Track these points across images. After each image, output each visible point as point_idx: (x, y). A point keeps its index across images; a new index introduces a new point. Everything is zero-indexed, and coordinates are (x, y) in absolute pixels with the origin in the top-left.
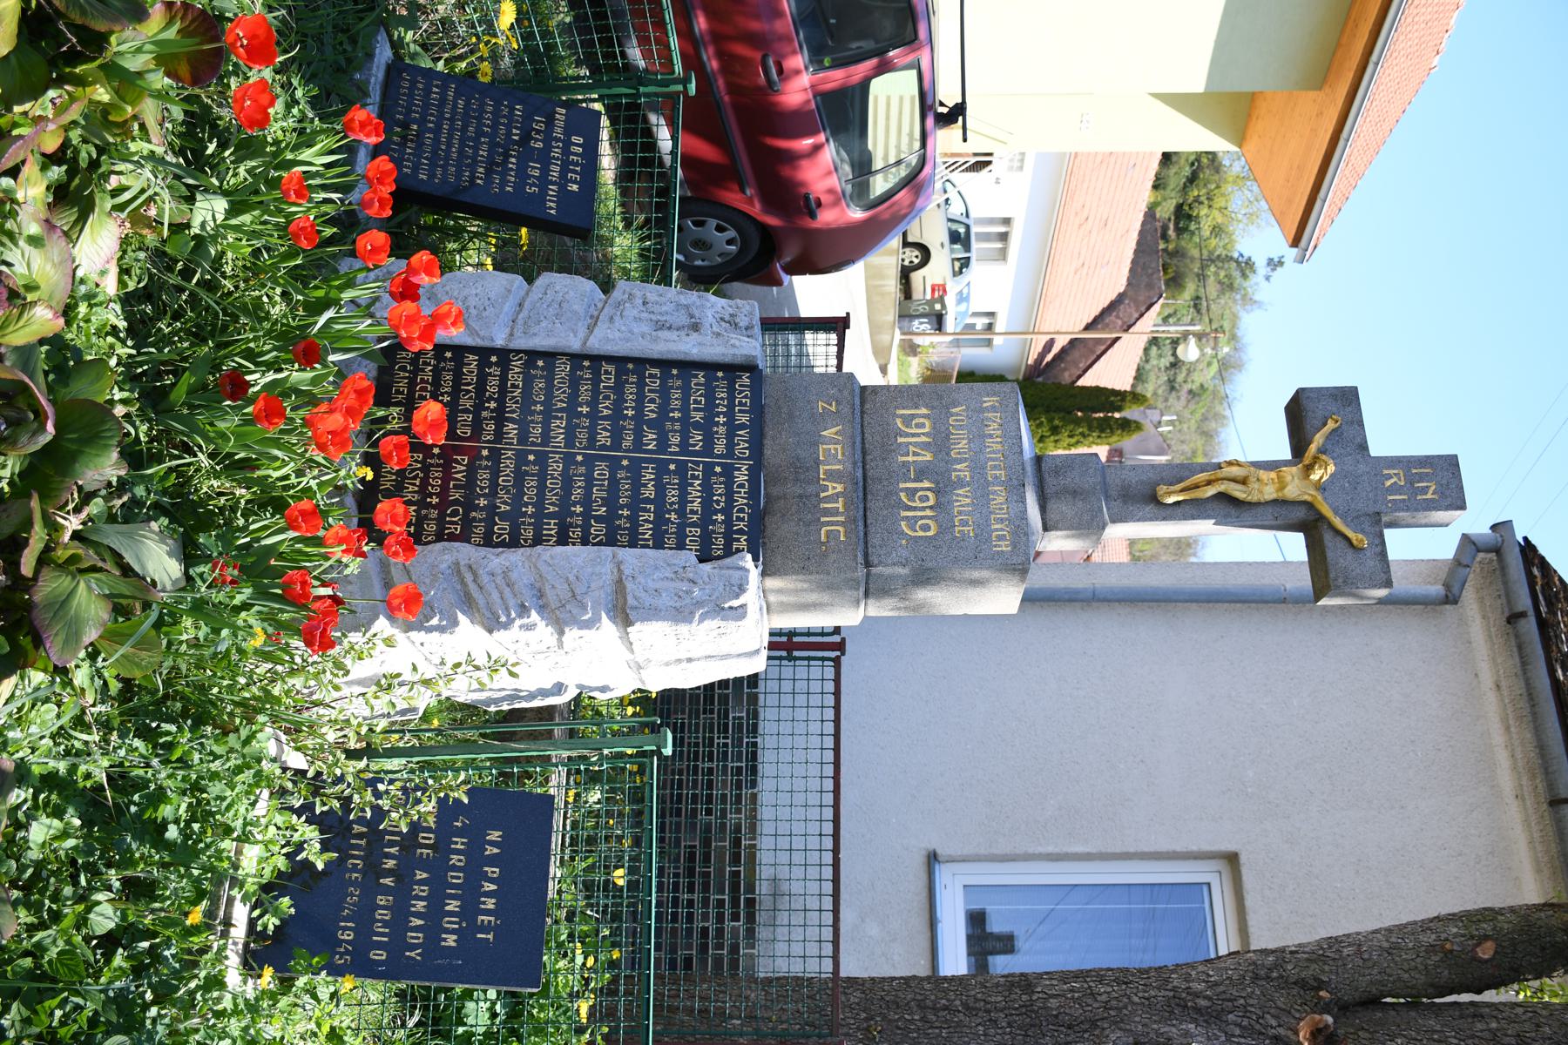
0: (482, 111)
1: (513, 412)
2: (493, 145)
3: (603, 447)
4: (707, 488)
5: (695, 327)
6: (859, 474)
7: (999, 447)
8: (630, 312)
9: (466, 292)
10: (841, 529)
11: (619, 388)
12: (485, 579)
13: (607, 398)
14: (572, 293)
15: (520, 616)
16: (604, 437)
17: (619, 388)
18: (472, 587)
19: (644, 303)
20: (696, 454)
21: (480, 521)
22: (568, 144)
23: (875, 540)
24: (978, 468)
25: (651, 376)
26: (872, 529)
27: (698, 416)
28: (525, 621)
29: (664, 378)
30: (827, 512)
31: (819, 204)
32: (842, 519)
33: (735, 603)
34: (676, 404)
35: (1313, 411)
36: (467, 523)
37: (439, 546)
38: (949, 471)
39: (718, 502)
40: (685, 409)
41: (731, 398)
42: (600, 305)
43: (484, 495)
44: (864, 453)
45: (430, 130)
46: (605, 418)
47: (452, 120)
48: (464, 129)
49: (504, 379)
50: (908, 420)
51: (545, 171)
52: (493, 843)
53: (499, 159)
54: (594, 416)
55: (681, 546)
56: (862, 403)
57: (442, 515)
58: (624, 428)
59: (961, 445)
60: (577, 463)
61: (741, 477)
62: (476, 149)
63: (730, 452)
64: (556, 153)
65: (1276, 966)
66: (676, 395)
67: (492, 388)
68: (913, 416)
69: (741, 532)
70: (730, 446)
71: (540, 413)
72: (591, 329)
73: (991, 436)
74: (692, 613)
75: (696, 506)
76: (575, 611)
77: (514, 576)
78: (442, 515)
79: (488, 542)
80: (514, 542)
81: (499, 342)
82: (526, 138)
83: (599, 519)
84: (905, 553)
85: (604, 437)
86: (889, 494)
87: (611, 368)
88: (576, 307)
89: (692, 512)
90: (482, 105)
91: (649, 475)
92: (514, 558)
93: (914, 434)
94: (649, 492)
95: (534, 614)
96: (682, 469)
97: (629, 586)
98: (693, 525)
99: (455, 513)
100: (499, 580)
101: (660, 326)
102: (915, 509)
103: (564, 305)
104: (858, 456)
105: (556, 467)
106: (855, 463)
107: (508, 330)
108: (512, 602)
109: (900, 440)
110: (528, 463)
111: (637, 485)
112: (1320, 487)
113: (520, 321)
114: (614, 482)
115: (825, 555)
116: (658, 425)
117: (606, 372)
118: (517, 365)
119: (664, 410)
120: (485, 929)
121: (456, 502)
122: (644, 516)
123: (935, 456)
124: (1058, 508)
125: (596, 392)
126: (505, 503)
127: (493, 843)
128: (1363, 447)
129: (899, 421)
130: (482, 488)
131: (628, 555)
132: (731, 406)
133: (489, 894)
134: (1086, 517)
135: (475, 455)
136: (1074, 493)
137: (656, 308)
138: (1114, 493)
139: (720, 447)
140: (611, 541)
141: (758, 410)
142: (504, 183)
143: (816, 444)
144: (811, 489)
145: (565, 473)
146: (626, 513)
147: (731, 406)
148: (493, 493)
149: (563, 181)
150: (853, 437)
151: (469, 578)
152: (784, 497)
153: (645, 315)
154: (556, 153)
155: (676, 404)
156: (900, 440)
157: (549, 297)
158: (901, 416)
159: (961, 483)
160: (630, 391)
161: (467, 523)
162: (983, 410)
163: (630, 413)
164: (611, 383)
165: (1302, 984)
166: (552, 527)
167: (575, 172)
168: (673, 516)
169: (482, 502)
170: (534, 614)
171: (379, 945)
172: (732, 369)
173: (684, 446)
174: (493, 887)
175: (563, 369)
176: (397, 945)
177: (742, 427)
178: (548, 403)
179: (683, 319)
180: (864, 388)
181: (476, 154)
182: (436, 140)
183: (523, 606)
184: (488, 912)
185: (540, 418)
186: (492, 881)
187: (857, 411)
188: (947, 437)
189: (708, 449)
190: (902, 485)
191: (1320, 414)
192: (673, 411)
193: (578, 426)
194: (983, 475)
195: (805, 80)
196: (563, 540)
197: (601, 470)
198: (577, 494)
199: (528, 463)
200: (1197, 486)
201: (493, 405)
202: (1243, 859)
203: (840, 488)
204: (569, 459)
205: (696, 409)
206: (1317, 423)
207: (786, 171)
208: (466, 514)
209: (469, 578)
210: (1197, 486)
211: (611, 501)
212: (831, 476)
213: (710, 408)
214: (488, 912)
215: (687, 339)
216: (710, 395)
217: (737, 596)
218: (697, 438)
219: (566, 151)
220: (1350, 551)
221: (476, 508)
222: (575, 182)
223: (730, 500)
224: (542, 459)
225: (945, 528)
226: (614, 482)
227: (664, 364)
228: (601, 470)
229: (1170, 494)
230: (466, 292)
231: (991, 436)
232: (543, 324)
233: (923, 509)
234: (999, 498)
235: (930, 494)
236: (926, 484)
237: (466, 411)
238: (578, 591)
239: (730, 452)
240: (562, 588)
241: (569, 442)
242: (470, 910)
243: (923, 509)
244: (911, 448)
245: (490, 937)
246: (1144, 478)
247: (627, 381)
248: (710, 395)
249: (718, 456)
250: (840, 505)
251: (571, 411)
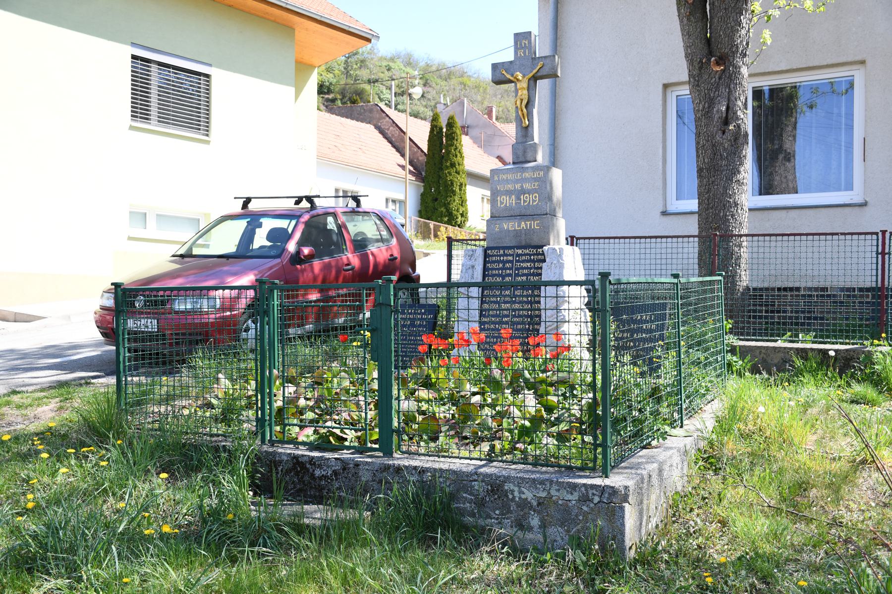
4: (523, 261)
5: (473, 267)
23: (539, 212)
24: (517, 181)
27: (501, 265)
29: (488, 275)
31: (392, 255)
41: (495, 256)
50: (502, 203)
55: (541, 268)
59: (510, 187)
61: (520, 251)
63: (513, 255)
65: (694, 78)
66: (494, 272)
70: (510, 255)
75: (529, 264)
93: (506, 201)
96: (517, 269)
105: (517, 306)
112: (524, 76)
116: (503, 277)
124: (529, 158)
128: (511, 62)
132: (497, 256)
136: (525, 152)
139: (511, 258)
141: (499, 248)
143: (509, 231)
147: (497, 256)
159: (522, 186)
165: (700, 68)
172: (486, 255)
173: (510, 269)
175: (486, 306)
189: (511, 262)
195: (350, 255)
198: (525, 299)
202: (666, 82)
207: (380, 268)
212: (519, 226)
213: (498, 262)
216: (494, 262)
218: (507, 265)
223: (527, 254)
224: (514, 310)
225: (535, 191)
234: (527, 175)
239: (513, 255)
248: (494, 262)
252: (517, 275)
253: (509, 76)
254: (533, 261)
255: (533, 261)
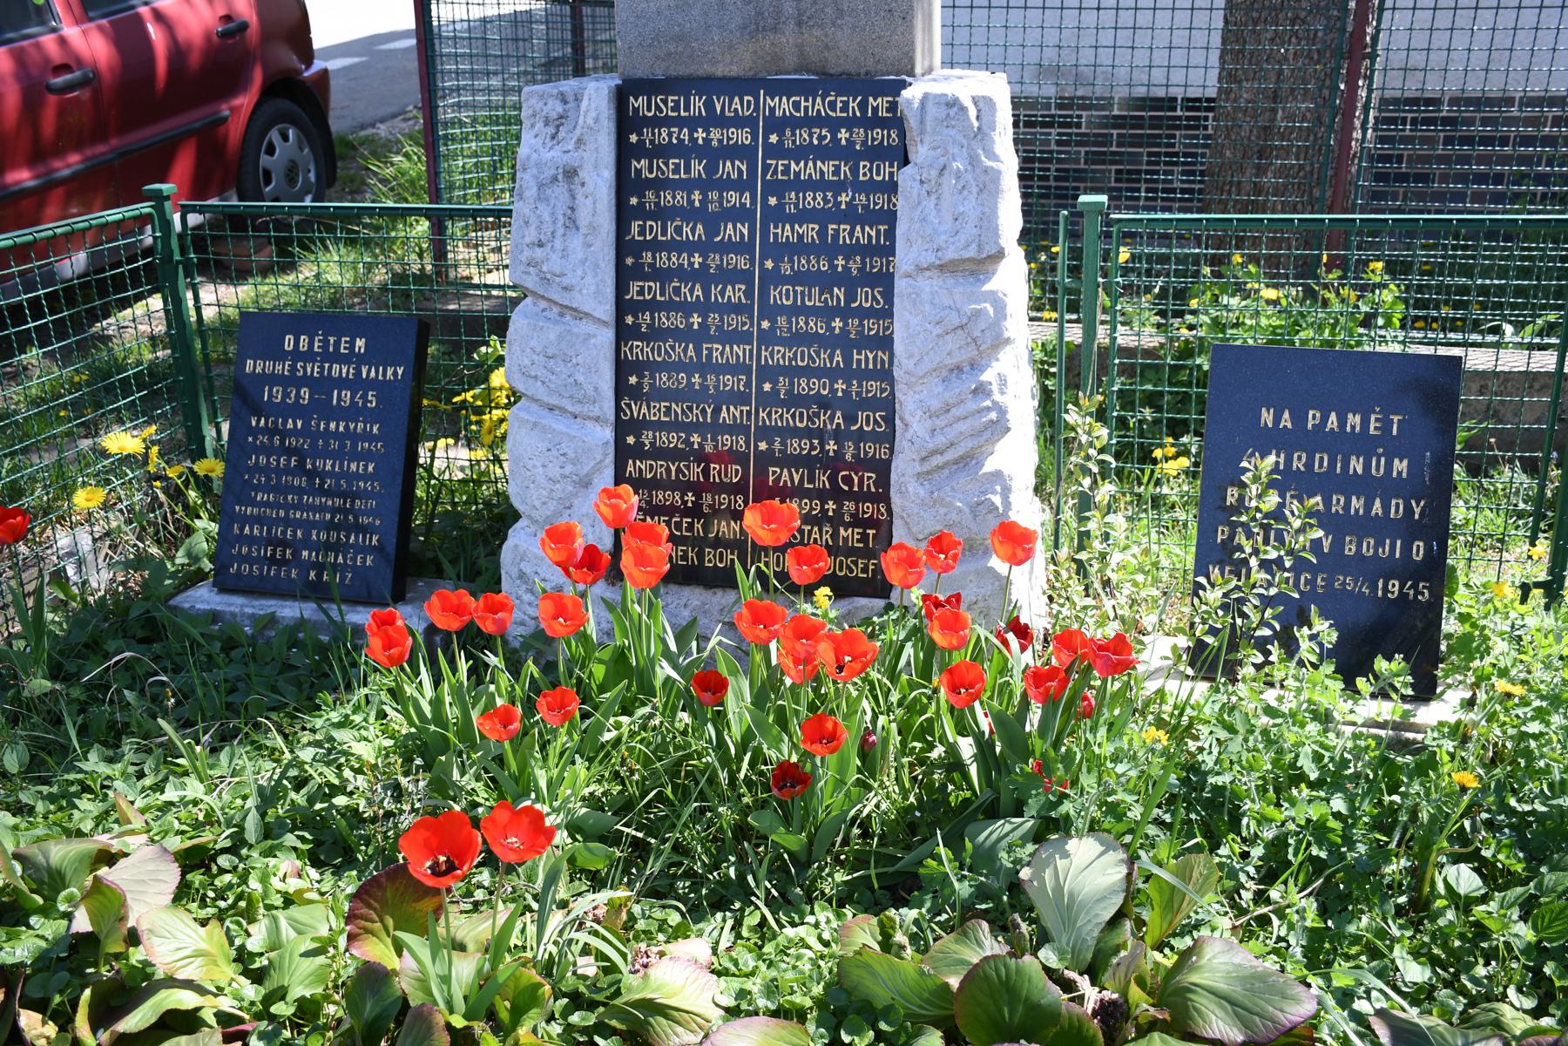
0: (265, 470)
1: (704, 411)
3: (749, 294)
4: (801, 153)
5: (571, 174)
8: (554, 263)
9: (541, 479)
11: (662, 276)
12: (940, 440)
13: (677, 291)
15: (989, 394)
16: (735, 293)
17: (662, 276)
18: (950, 455)
19: (541, 245)
22: (296, 355)
25: (642, 232)
27: (697, 168)
28: (995, 388)
29: (641, 213)
31: (227, 18)
33: (972, 112)
34: (681, 198)
37: (896, 499)
39: (821, 138)
40: (688, 186)
41: (667, 122)
42: (543, 304)
43: (822, 444)
45: (307, 535)
47: (288, 507)
48: (300, 491)
49: (659, 426)
51: (342, 383)
54: (704, 308)
55: (891, 187)
57: (850, 495)
58: (719, 267)
60: (773, 328)
61: (783, 106)
63: (750, 122)
64: (313, 369)
67: (672, 440)
70: (738, 122)
72: (580, 315)
74: (986, 170)
75: (827, 168)
76: (983, 325)
77: (935, 404)
78: (850, 495)
79: (889, 437)
80: (888, 406)
81: (608, 434)
82: (296, 410)
83: (851, 297)
85: (735, 293)
87: (634, 287)
88: (552, 336)
91: (786, 232)
92: (910, 404)
95: (985, 377)
96: (773, 187)
97: (950, 255)
98: (855, 171)
100: (939, 422)
101: (572, 223)
103: (550, 352)
105: (780, 355)
107: (589, 424)
108: (971, 406)
110: (775, 391)
111: (800, 248)
113: (576, 409)
114: (798, 278)
117: (641, 292)
118: (637, 410)
119: (690, 214)
120: (1386, 425)
121: (833, 479)
125: (669, 306)
126: (832, 418)
130: (812, 448)
131: (904, 259)
132: (680, 122)
133: (1342, 422)
135: (765, 460)
139: (742, 136)
140: (885, 281)
145: (787, 343)
146: (840, 262)
147: (680, 122)
148: (821, 434)
149: (350, 358)
151: (938, 460)
152: (800, 47)
153: (558, 244)
154: (313, 369)
157: (541, 372)
160: (664, 260)
161: (860, 464)
163: (697, 259)
166: (865, 358)
167: (337, 344)
168: (844, 198)
170: (985, 377)
171: (1407, 549)
172: (625, 122)
173: (740, 185)
174: (1333, 417)
175: (638, 350)
181: (331, 474)
183: (975, 392)
184: (1365, 423)
186: (1325, 419)
193: (719, 328)
195: (71, 32)
196: (886, 343)
198: (816, 326)
199: (775, 391)
201: (696, 438)
204: (767, 338)
205: (687, 171)
207: (195, 59)
208: (850, 467)
209: (938, 460)
211: (826, 282)
214: (1365, 423)
215: (590, 186)
217: (964, 109)
218: (728, 168)
219: (309, 356)
221: (839, 453)
222: (352, 343)
223: (819, 121)
224: (767, 372)
226: (798, 278)
227: (623, 216)
228: (780, 296)
230: (541, 479)
232: (581, 379)
237: (706, 472)
238: (956, 322)
239: (750, 122)
240: (951, 343)
241: (745, 338)
242: (1362, 444)
245: (1396, 418)
247: (652, 266)
251: (701, 336)
252: (776, 215)
254: (847, 154)
255: (847, 154)
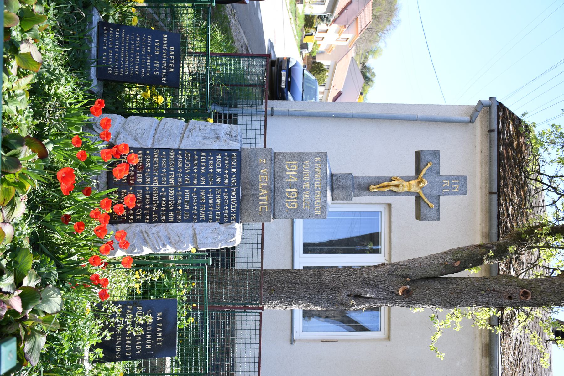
0: (135, 40)
1: (156, 172)
2: (141, 55)
3: (187, 184)
4: (222, 197)
5: (218, 138)
6: (273, 186)
7: (319, 177)
8: (195, 133)
9: (136, 127)
10: (266, 207)
11: (191, 161)
12: (151, 236)
13: (188, 165)
14: (174, 126)
15: (163, 247)
16: (187, 181)
17: (191, 161)
18: (147, 238)
19: (199, 130)
20: (218, 185)
21: (148, 214)
22: (169, 50)
23: (277, 210)
24: (312, 184)
25: (203, 156)
26: (276, 206)
27: (219, 171)
28: (165, 249)
29: (207, 156)
30: (262, 200)
32: (266, 203)
33: (232, 240)
34: (211, 166)
35: (425, 158)
36: (144, 215)
37: (135, 225)
38: (302, 185)
39: (226, 202)
40: (214, 168)
41: (230, 163)
42: (184, 128)
43: (148, 204)
44: (274, 178)
45: (117, 52)
46: (187, 173)
47: (125, 46)
48: (129, 50)
49: (152, 160)
50: (289, 166)
51: (161, 64)
52: (159, 316)
53: (143, 61)
54: (183, 172)
55: (214, 221)
56: (274, 159)
57: (135, 212)
58: (194, 177)
59: (307, 176)
60: (178, 191)
61: (234, 193)
62: (135, 58)
63: (230, 184)
64: (165, 55)
65: (395, 270)
66: (211, 163)
67: (148, 164)
68: (291, 164)
69: (233, 213)
70: (230, 181)
71: (165, 172)
72: (182, 139)
73: (317, 172)
74: (218, 244)
75: (219, 204)
76: (181, 245)
77: (160, 234)
78: (135, 212)
79: (151, 222)
80: (159, 221)
81: (149, 146)
82: (153, 50)
83: (187, 211)
84: (286, 214)
85: (187, 181)
86: (282, 193)
87: (188, 154)
88: (176, 132)
89: (218, 206)
90: (136, 37)
91: (203, 194)
92: (161, 227)
93: (291, 171)
94: (203, 200)
95: (168, 246)
96: (214, 191)
97: (198, 237)
98: (218, 211)
99: (139, 211)
100: (156, 235)
101: (205, 138)
102: (290, 199)
103: (172, 131)
104: (272, 180)
105: (172, 193)
106: (271, 183)
107: (152, 141)
108: (160, 243)
109: (287, 173)
110: (162, 192)
111: (199, 197)
112: (421, 188)
113: (156, 137)
114: (191, 197)
115: (261, 216)
116: (205, 175)
117: (187, 155)
118: (156, 154)
119: (207, 169)
120: (159, 342)
121: (139, 207)
122: (202, 209)
123: (298, 179)
124: (337, 193)
125: (184, 163)
126: (155, 207)
127: (159, 316)
128: (438, 173)
129: (286, 166)
130: (147, 202)
131: (198, 225)
132: (230, 166)
133: (159, 332)
134: (346, 196)
135: (144, 189)
136: (343, 188)
137: (204, 132)
138: (356, 187)
140: (190, 220)
141: (239, 167)
142: (146, 73)
143: (258, 175)
144: (256, 192)
145: (175, 195)
146: (196, 208)
147: (230, 166)
148: (151, 203)
149: (168, 67)
150: (271, 173)
151: (146, 235)
152: (248, 195)
153: (200, 134)
154: (165, 55)
155: (211, 166)
156: (287, 173)
157: (166, 128)
158: (287, 164)
159: (306, 190)
160: (196, 161)
161: (144, 215)
162: (315, 163)
163: (196, 171)
164: (189, 159)
165: (402, 276)
166: (171, 215)
167: (172, 63)
168: (211, 208)
169: (148, 207)
170: (168, 246)
171: (129, 351)
172: (231, 152)
173: (214, 182)
174: (161, 329)
176: (133, 350)
177: (234, 174)
178: (167, 168)
179: (214, 135)
180: (275, 153)
181: (135, 60)
182: (120, 57)
183: (164, 244)
184: (159, 337)
185: (165, 174)
186: (160, 327)
187: (273, 163)
188: (302, 173)
189: (222, 183)
190: (287, 190)
191: (426, 160)
192: (210, 169)
193: (178, 177)
194: (313, 187)
196: (175, 221)
197: (187, 192)
199: (162, 192)
200: (383, 187)
201: (149, 170)
202: (392, 206)
203: (266, 192)
204: (176, 189)
205: (218, 168)
206: (425, 164)
208: (143, 212)
209: (146, 235)
210: (383, 187)
211: (190, 204)
212: (263, 187)
213: (223, 168)
214: (159, 337)
215: (214, 144)
216: (223, 162)
217: (233, 238)
218: (219, 179)
219: (168, 55)
220: (428, 208)
221: (146, 209)
222: (172, 68)
223: (230, 201)
224: (167, 189)
225: (300, 206)
226: (191, 197)
227: (207, 151)
228: (187, 192)
229: (374, 188)
230: (136, 127)
231: (317, 172)
232: (164, 139)
233: (293, 199)
234: (318, 195)
235: (295, 193)
236: (294, 190)
237: (140, 173)
238: (181, 238)
239: (230, 184)
240: (176, 238)
241: (176, 183)
242: (154, 336)
243: (293, 199)
244: (290, 176)
245: (161, 344)
246: (366, 181)
247: (194, 159)
248: (223, 162)
249: (226, 186)
250: (266, 198)
251: (176, 171)
252: (207, 191)
253: (424, 171)
254: (222, 209)
255: (222, 209)
